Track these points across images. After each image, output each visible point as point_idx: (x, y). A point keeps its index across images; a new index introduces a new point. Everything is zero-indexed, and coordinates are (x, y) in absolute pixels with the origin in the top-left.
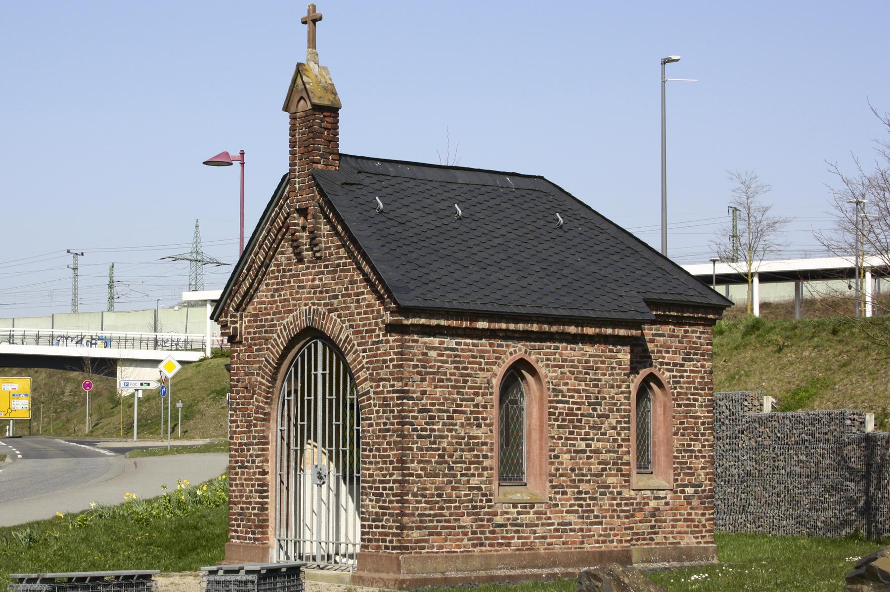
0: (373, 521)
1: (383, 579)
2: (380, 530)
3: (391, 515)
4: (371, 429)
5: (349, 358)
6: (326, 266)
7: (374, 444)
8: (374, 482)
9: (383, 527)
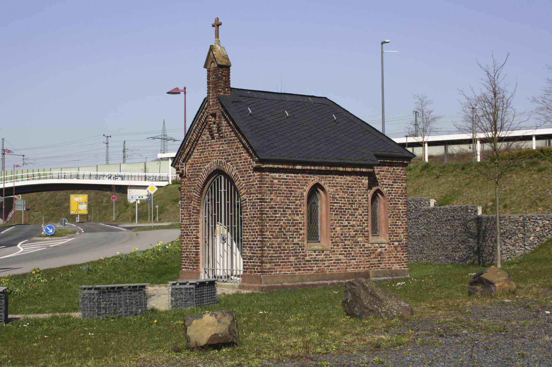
0: (249, 259)
3: (257, 257)
5: (236, 184)
6: (225, 141)
7: (249, 223)
8: (249, 241)
9: (253, 262)
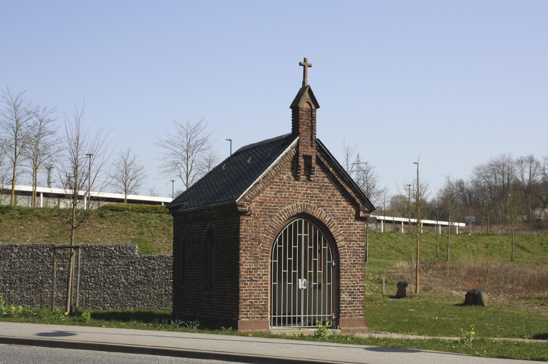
3: (359, 301)
5: (332, 230)
8: (348, 287)
9: (354, 306)
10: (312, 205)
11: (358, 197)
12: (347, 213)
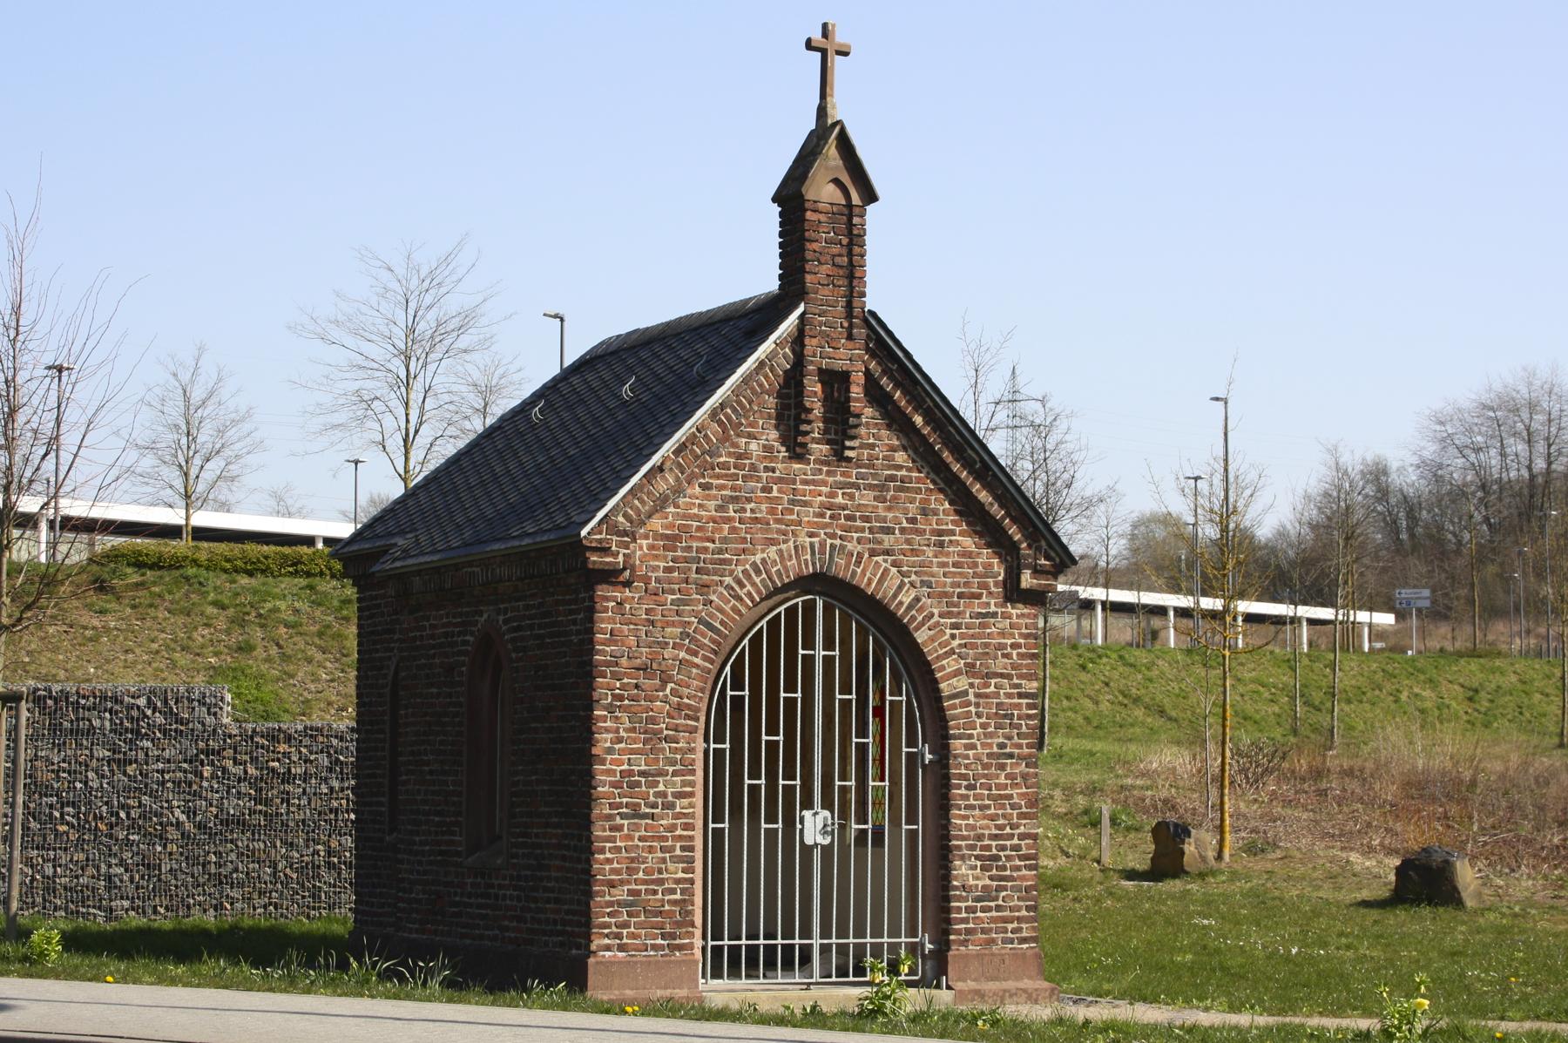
1: (1025, 991)
2: (994, 914)
4: (971, 753)
5: (921, 636)
8: (980, 838)
10: (850, 546)
11: (1014, 520)
12: (975, 575)
